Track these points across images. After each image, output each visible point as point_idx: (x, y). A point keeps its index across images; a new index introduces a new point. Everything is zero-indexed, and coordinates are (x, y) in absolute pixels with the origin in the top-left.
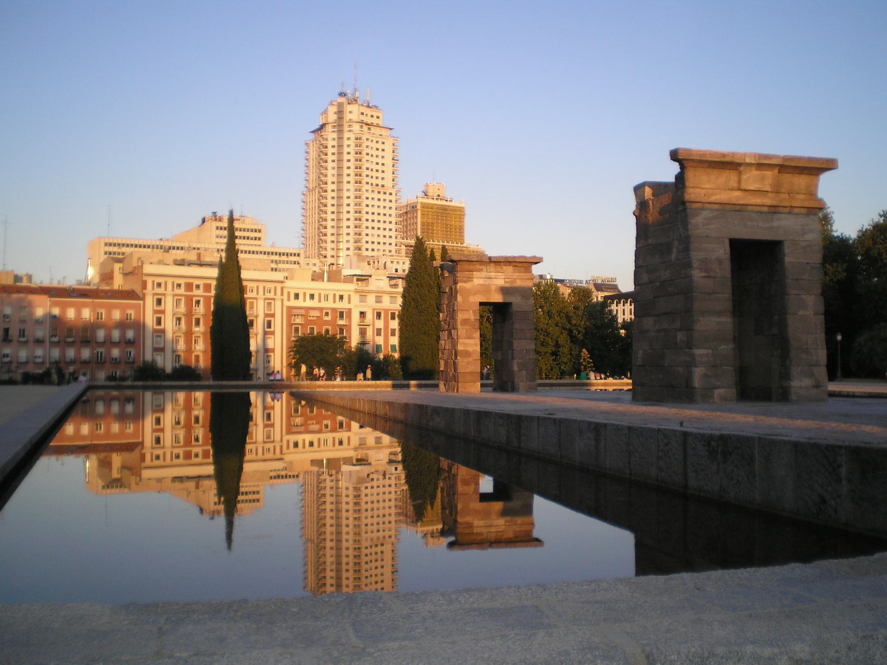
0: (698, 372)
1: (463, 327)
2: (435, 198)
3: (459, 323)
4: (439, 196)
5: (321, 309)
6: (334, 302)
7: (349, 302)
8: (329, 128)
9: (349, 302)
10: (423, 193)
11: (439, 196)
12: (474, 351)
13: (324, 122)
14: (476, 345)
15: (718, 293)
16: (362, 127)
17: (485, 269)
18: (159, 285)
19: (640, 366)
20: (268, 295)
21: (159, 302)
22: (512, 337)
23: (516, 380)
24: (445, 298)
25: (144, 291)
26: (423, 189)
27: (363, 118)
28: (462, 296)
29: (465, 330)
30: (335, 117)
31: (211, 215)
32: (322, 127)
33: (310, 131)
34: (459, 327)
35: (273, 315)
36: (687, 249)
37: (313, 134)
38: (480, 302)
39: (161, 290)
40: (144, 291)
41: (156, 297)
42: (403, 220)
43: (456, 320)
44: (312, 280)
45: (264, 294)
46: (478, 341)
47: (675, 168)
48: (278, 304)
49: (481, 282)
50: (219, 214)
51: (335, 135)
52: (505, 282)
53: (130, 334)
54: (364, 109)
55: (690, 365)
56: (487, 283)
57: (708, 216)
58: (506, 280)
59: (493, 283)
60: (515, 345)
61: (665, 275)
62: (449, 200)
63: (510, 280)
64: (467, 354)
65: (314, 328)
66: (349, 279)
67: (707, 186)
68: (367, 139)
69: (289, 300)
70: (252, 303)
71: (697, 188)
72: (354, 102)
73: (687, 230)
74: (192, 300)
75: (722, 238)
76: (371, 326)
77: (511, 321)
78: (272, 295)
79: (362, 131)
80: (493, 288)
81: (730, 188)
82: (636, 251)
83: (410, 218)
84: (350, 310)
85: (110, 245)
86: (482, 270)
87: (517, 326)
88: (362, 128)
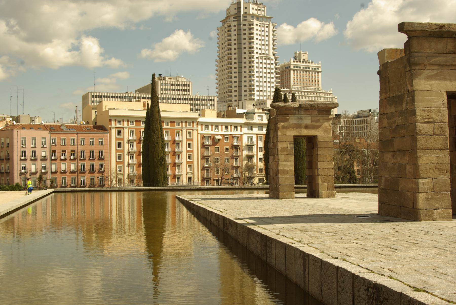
0: (422, 197)
1: (282, 154)
2: (301, 61)
3: (279, 150)
4: (304, 60)
5: (223, 136)
6: (231, 131)
7: (241, 131)
8: (232, 19)
9: (241, 131)
10: (294, 59)
11: (304, 60)
12: (291, 170)
13: (229, 14)
14: (291, 165)
15: (437, 135)
17: (297, 112)
19: (383, 189)
20: (188, 127)
21: (119, 132)
22: (317, 160)
23: (320, 190)
24: (272, 133)
26: (294, 56)
28: (281, 132)
29: (283, 156)
30: (236, 11)
32: (228, 17)
34: (279, 153)
35: (192, 140)
36: (413, 101)
38: (294, 136)
39: (121, 126)
42: (281, 76)
43: (277, 149)
44: (217, 117)
45: (186, 126)
46: (293, 163)
47: (404, 37)
48: (195, 132)
49: (295, 121)
50: (163, 76)
51: (236, 23)
52: (312, 121)
55: (416, 191)
56: (299, 122)
57: (429, 74)
58: (312, 120)
59: (304, 122)
60: (319, 165)
61: (399, 121)
62: (311, 62)
63: (315, 120)
64: (285, 172)
65: (218, 147)
66: (240, 116)
67: (429, 51)
69: (202, 130)
70: (178, 133)
71: (419, 53)
73: (412, 86)
74: (141, 132)
75: (441, 91)
76: (255, 146)
77: (317, 148)
78: (191, 127)
80: (303, 125)
81: (447, 52)
82: (380, 102)
83: (285, 75)
84: (242, 135)
86: (295, 113)
87: (320, 152)
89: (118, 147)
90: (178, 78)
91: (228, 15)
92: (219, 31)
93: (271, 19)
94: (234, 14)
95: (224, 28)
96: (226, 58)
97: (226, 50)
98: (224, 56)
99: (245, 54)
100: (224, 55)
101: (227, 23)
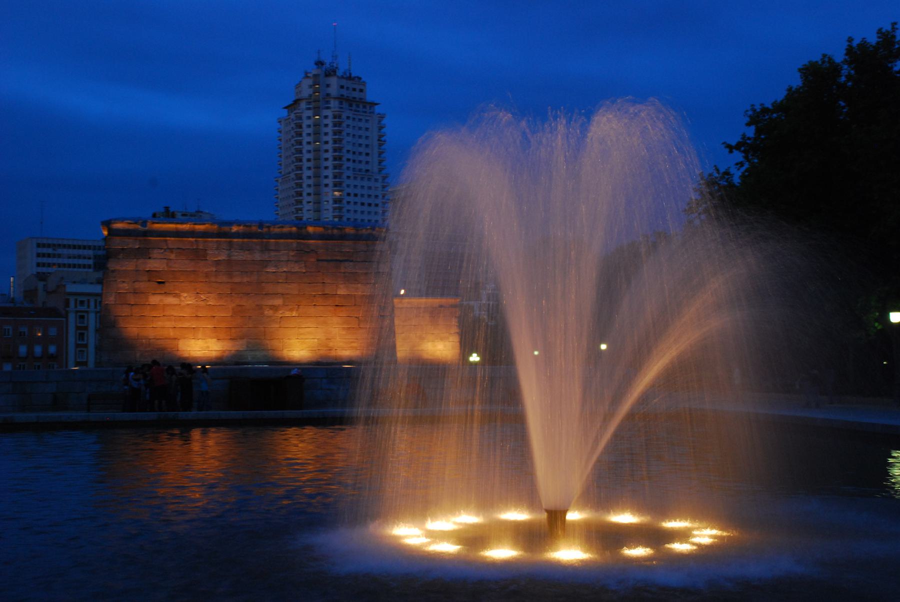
8: (303, 105)
16: (341, 103)
18: (82, 303)
25: (67, 309)
27: (344, 92)
31: (162, 210)
32: (296, 102)
33: (283, 107)
37: (286, 110)
39: (85, 308)
40: (67, 309)
41: (79, 314)
50: (171, 210)
53: (52, 349)
54: (344, 82)
68: (348, 118)
72: (332, 73)
79: (341, 108)
85: (44, 246)
88: (342, 105)
89: (79, 340)
90: (200, 214)
91: (297, 98)
92: (281, 124)
93: (376, 107)
94: (307, 95)
95: (290, 120)
96: (292, 176)
97: (293, 161)
98: (289, 173)
99: (326, 171)
100: (290, 169)
101: (295, 112)
